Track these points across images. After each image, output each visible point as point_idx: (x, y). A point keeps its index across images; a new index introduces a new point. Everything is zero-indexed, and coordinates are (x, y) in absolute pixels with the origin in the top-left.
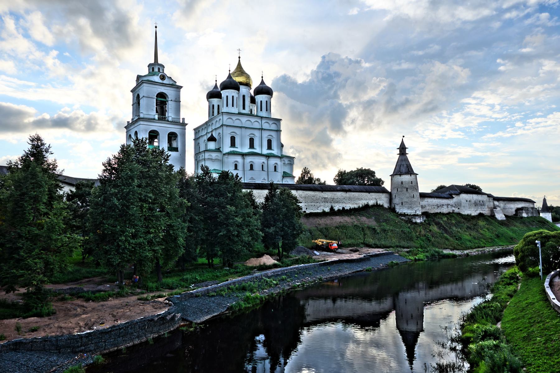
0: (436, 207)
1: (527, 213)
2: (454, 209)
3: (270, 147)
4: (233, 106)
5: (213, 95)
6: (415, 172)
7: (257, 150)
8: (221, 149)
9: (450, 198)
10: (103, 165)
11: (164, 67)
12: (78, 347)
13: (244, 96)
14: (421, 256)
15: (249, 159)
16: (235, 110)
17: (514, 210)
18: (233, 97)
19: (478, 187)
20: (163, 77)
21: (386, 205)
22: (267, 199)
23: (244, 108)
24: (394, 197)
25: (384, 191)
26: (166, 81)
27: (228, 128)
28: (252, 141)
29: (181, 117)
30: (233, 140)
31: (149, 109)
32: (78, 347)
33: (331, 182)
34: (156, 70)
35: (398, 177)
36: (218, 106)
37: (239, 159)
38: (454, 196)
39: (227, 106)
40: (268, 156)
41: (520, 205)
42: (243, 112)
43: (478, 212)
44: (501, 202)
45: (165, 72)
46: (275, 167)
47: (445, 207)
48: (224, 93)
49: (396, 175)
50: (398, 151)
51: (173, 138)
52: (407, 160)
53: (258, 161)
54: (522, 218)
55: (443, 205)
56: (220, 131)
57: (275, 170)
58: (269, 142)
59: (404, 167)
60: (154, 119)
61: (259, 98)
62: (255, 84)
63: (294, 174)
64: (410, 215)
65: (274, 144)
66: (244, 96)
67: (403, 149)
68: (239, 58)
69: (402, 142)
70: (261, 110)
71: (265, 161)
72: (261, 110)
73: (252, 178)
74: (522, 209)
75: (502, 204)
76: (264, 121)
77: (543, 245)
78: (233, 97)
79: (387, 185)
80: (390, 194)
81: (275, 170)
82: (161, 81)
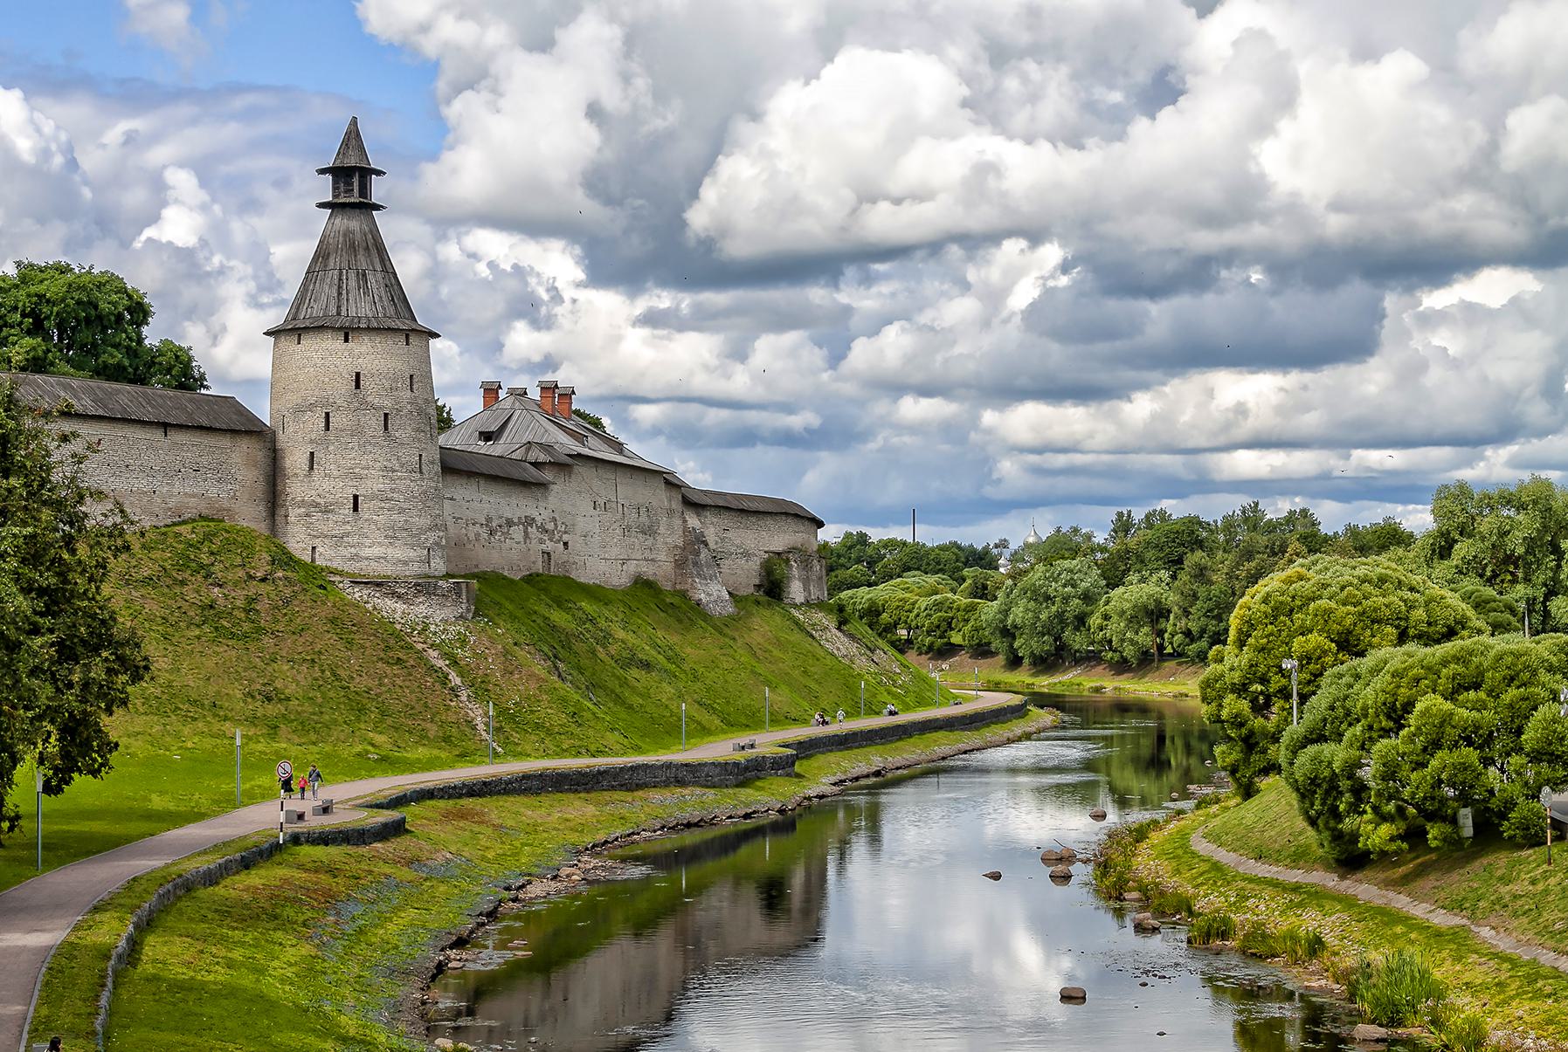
2: (549, 546)
9: (525, 484)
17: (755, 565)
41: (779, 538)
43: (632, 568)
44: (709, 517)
47: (517, 532)
50: (324, 188)
55: (510, 523)
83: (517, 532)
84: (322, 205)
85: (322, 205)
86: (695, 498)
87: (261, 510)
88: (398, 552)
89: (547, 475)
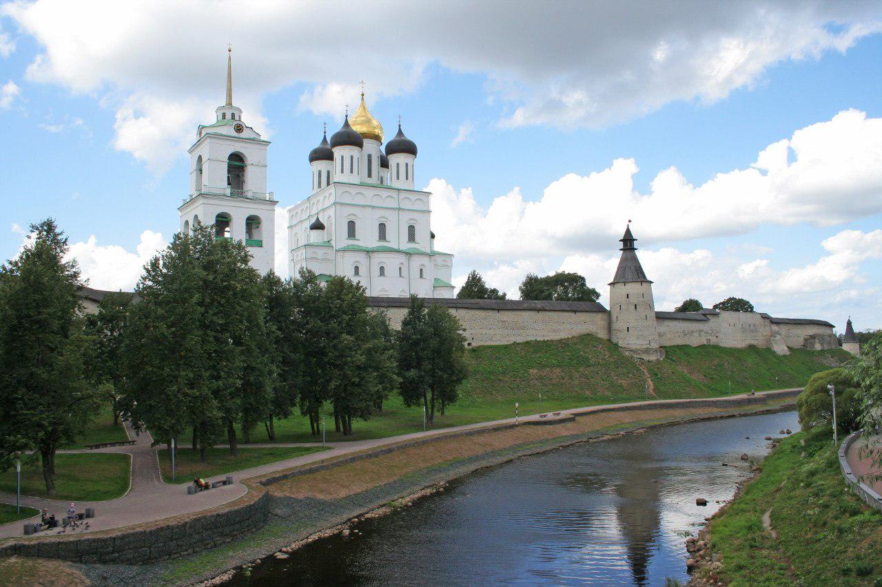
0: (682, 335)
1: (822, 344)
2: (709, 337)
3: (412, 238)
4: (352, 172)
5: (322, 154)
6: (649, 278)
7: (392, 242)
8: (333, 243)
10: (145, 268)
11: (241, 112)
12: (109, 553)
13: (370, 156)
15: (378, 259)
16: (355, 179)
18: (352, 157)
20: (239, 129)
21: (602, 334)
22: (405, 323)
23: (370, 175)
24: (614, 318)
25: (601, 309)
26: (242, 135)
27: (344, 208)
28: (382, 227)
29: (268, 191)
30: (352, 225)
31: (217, 177)
32: (109, 553)
33: (514, 294)
34: (228, 116)
36: (328, 172)
37: (361, 258)
39: (342, 172)
40: (408, 254)
42: (369, 181)
43: (748, 342)
45: (242, 120)
46: (421, 270)
47: (696, 335)
48: (338, 152)
50: (621, 245)
51: (254, 226)
52: (635, 259)
53: (392, 262)
55: (693, 332)
56: (331, 212)
57: (421, 276)
58: (412, 229)
59: (631, 271)
60: (224, 195)
61: (394, 159)
62: (388, 137)
63: (453, 284)
65: (420, 234)
66: (370, 156)
68: (363, 95)
69: (628, 232)
70: (398, 178)
71: (406, 263)
72: (398, 178)
73: (383, 290)
74: (813, 337)
75: (783, 329)
76: (403, 195)
77: (838, 393)
78: (352, 157)
79: (605, 300)
80: (609, 313)
81: (421, 276)
82: (236, 134)
84: (620, 250)
85: (620, 250)
86: (775, 321)
87: (606, 332)
88: (638, 342)
89: (709, 317)
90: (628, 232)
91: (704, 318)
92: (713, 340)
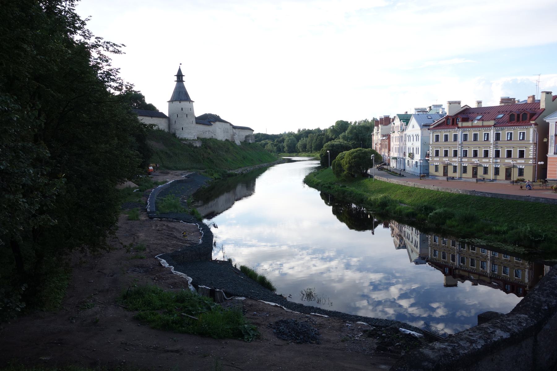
6: (192, 99)
9: (208, 125)
14: (216, 175)
17: (244, 137)
19: (218, 117)
35: (178, 103)
38: (212, 123)
41: (247, 133)
43: (225, 138)
44: (237, 130)
47: (207, 133)
49: (175, 101)
50: (176, 78)
54: (250, 143)
59: (181, 95)
64: (190, 140)
67: (180, 76)
83: (207, 133)
89: (212, 123)
90: (180, 71)
91: (208, 123)
92: (214, 137)
